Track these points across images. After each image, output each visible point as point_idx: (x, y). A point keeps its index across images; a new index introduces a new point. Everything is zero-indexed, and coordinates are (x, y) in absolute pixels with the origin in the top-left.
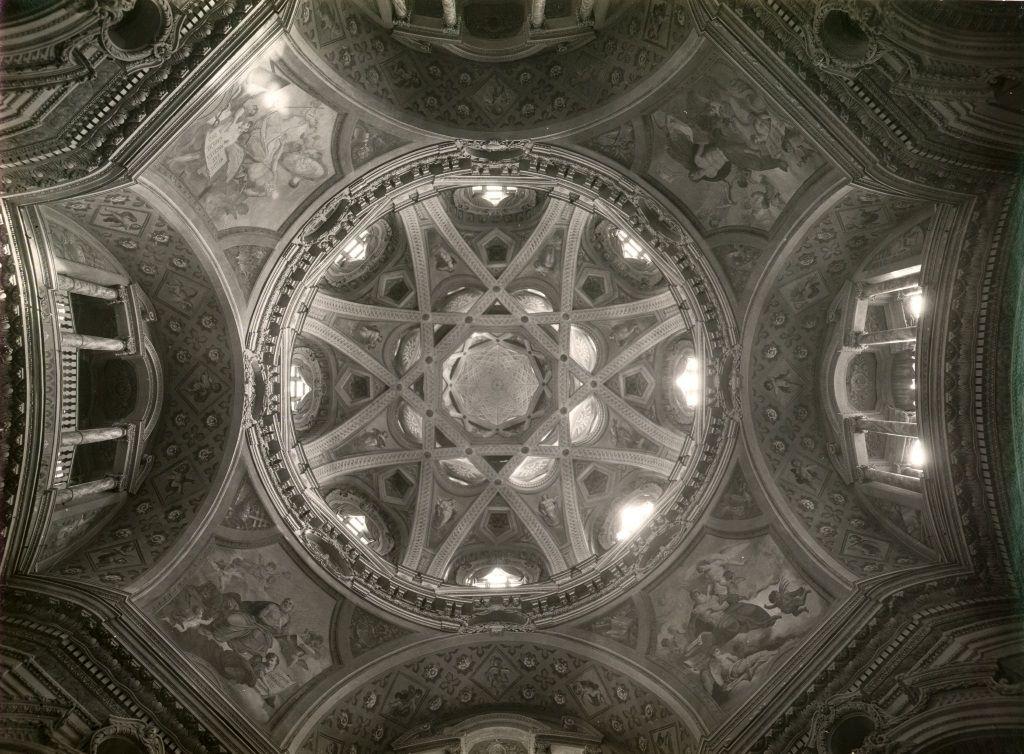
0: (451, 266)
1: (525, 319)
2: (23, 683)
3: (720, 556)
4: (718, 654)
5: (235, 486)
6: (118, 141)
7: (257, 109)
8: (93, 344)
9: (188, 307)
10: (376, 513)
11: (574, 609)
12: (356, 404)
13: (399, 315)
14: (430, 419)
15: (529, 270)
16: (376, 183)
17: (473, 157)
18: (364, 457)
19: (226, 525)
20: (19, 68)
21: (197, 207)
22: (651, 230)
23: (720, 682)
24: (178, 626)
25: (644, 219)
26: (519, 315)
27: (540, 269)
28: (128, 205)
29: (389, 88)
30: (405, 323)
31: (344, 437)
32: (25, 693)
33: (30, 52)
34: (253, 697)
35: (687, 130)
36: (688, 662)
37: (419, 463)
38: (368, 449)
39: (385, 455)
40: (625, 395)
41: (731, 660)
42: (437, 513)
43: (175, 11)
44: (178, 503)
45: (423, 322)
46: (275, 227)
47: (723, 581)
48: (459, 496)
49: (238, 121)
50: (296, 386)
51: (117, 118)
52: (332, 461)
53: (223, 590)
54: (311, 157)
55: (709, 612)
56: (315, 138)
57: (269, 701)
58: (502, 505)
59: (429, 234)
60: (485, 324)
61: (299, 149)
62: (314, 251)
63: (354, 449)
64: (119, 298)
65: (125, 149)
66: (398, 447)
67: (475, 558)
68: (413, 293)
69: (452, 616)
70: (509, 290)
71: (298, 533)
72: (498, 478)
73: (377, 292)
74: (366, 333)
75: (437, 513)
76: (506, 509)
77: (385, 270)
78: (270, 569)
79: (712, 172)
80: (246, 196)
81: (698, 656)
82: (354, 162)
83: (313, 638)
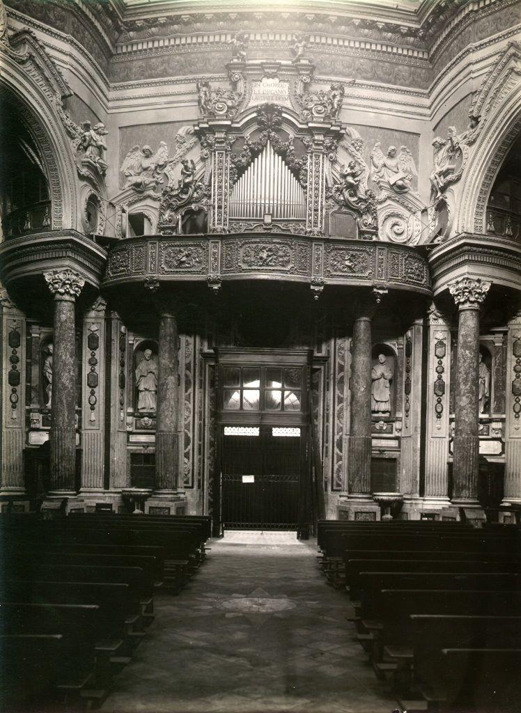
20: (47, 79)
33: (38, 84)
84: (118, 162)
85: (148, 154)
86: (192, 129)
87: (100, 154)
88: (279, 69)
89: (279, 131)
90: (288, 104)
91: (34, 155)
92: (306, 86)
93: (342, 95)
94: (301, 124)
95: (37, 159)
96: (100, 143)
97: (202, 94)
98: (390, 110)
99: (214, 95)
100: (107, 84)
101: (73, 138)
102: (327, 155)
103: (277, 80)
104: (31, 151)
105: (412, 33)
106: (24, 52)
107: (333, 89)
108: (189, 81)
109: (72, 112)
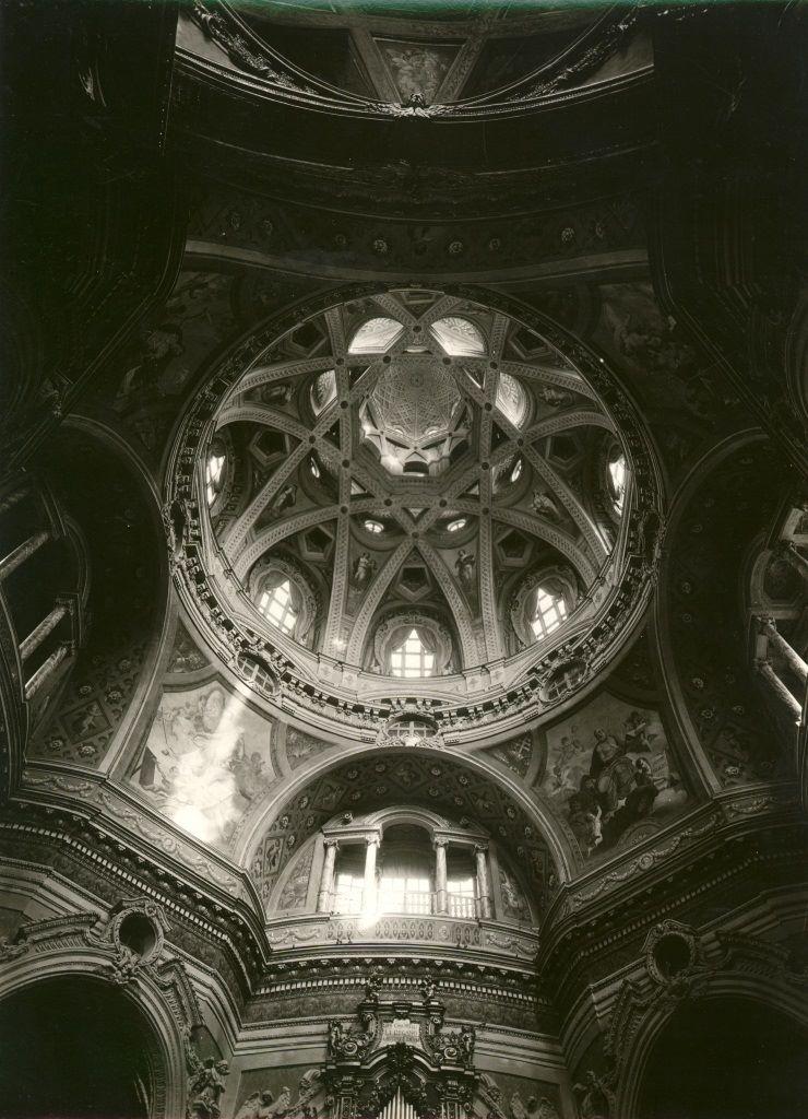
0: (290, 490)
1: (344, 405)
2: (605, 999)
5: (494, 761)
6: (218, 908)
8: (371, 854)
9: (341, 789)
10: (538, 574)
12: (429, 582)
13: (342, 545)
14: (448, 503)
15: (290, 409)
16: (219, 632)
18: (482, 586)
19: (524, 775)
20: (182, 1008)
21: (258, 801)
24: (598, 841)
26: (340, 411)
27: (288, 397)
28: (261, 858)
29: (135, 647)
30: (351, 532)
31: (461, 604)
32: (613, 999)
34: (666, 796)
35: (130, 375)
36: (727, 402)
37: (493, 520)
38: (473, 578)
39: (482, 559)
42: (544, 514)
43: (119, 908)
44: (502, 808)
45: (349, 512)
46: (269, 725)
47: (646, 337)
48: (530, 484)
49: (185, 782)
50: (411, 669)
51: (202, 913)
52: (482, 623)
54: (205, 705)
56: (188, 705)
57: (673, 783)
58: (546, 442)
59: (248, 400)
60: (350, 446)
61: (200, 718)
62: (287, 678)
63: (472, 592)
64: (335, 844)
65: (223, 901)
66: (475, 540)
67: (597, 494)
68: (322, 528)
70: (312, 427)
71: (540, 709)
72: (516, 442)
73: (319, 563)
74: (361, 573)
75: (544, 514)
77: (297, 555)
78: (567, 743)
79: (171, 339)
80: (245, 755)
82: (204, 666)
83: (633, 720)
84: (233, 1110)
85: (267, 1101)
86: (318, 1072)
87: (216, 1097)
88: (410, 1010)
89: (411, 1075)
90: (419, 1045)
91: (144, 1091)
92: (438, 1027)
93: (474, 1038)
94: (433, 1067)
95: (146, 1097)
96: (219, 1083)
97: (333, 1035)
98: (523, 1056)
99: (344, 1036)
100: (239, 1023)
101: (191, 1074)
102: (463, 1104)
103: (408, 1021)
104: (143, 1087)
105: (532, 979)
106: (169, 978)
107: (464, 1031)
108: (321, 1022)
109: (198, 1047)
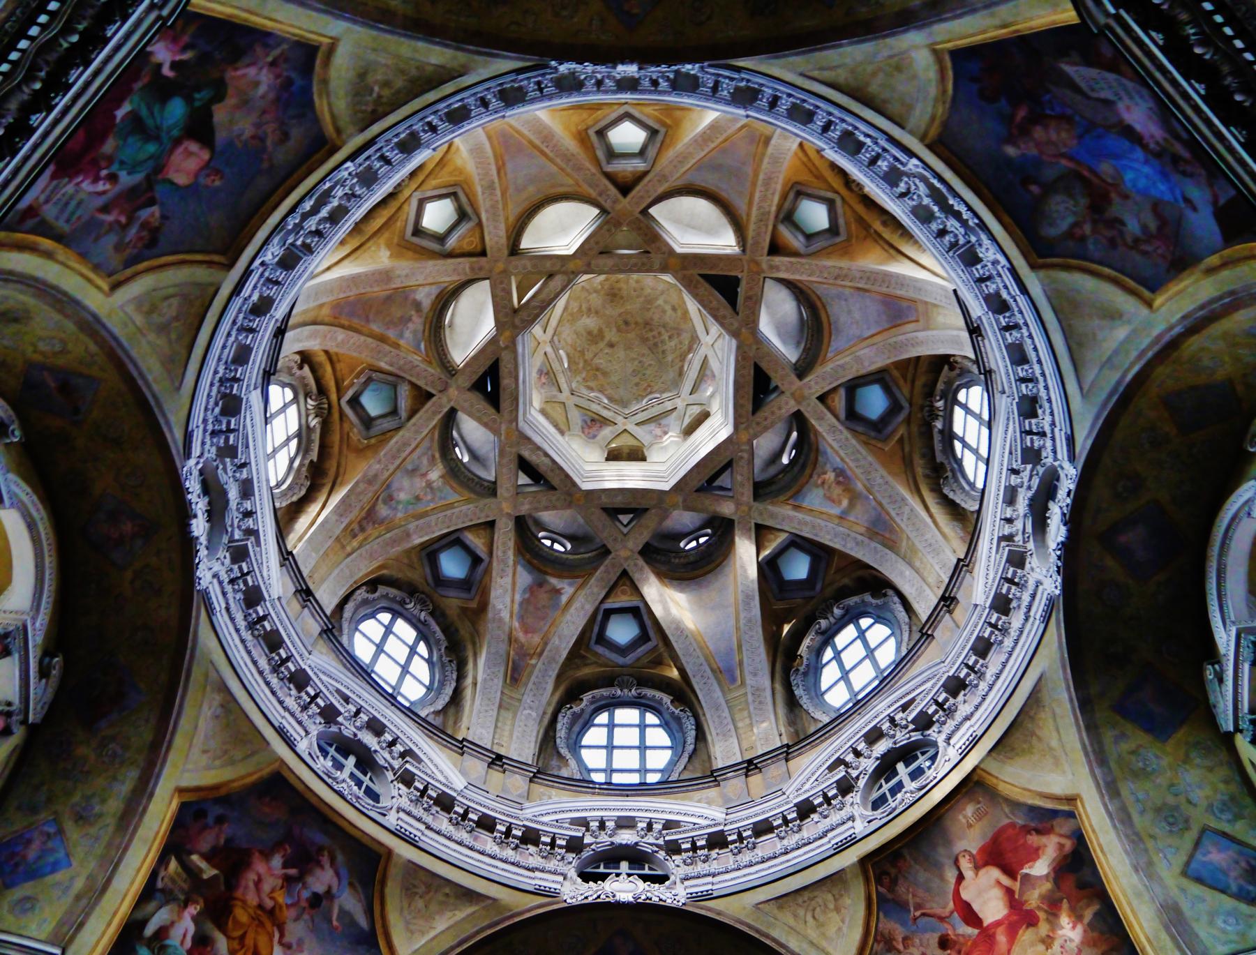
3: (345, 882)
4: (193, 910)
7: (1184, 173)
11: (243, 641)
17: (1041, 470)
22: (882, 747)
23: (149, 930)
25: (902, 738)
40: (606, 610)
41: (185, 936)
47: (306, 894)
53: (230, 74)
55: (256, 878)
69: (214, 433)
76: (404, 414)
81: (184, 876)
